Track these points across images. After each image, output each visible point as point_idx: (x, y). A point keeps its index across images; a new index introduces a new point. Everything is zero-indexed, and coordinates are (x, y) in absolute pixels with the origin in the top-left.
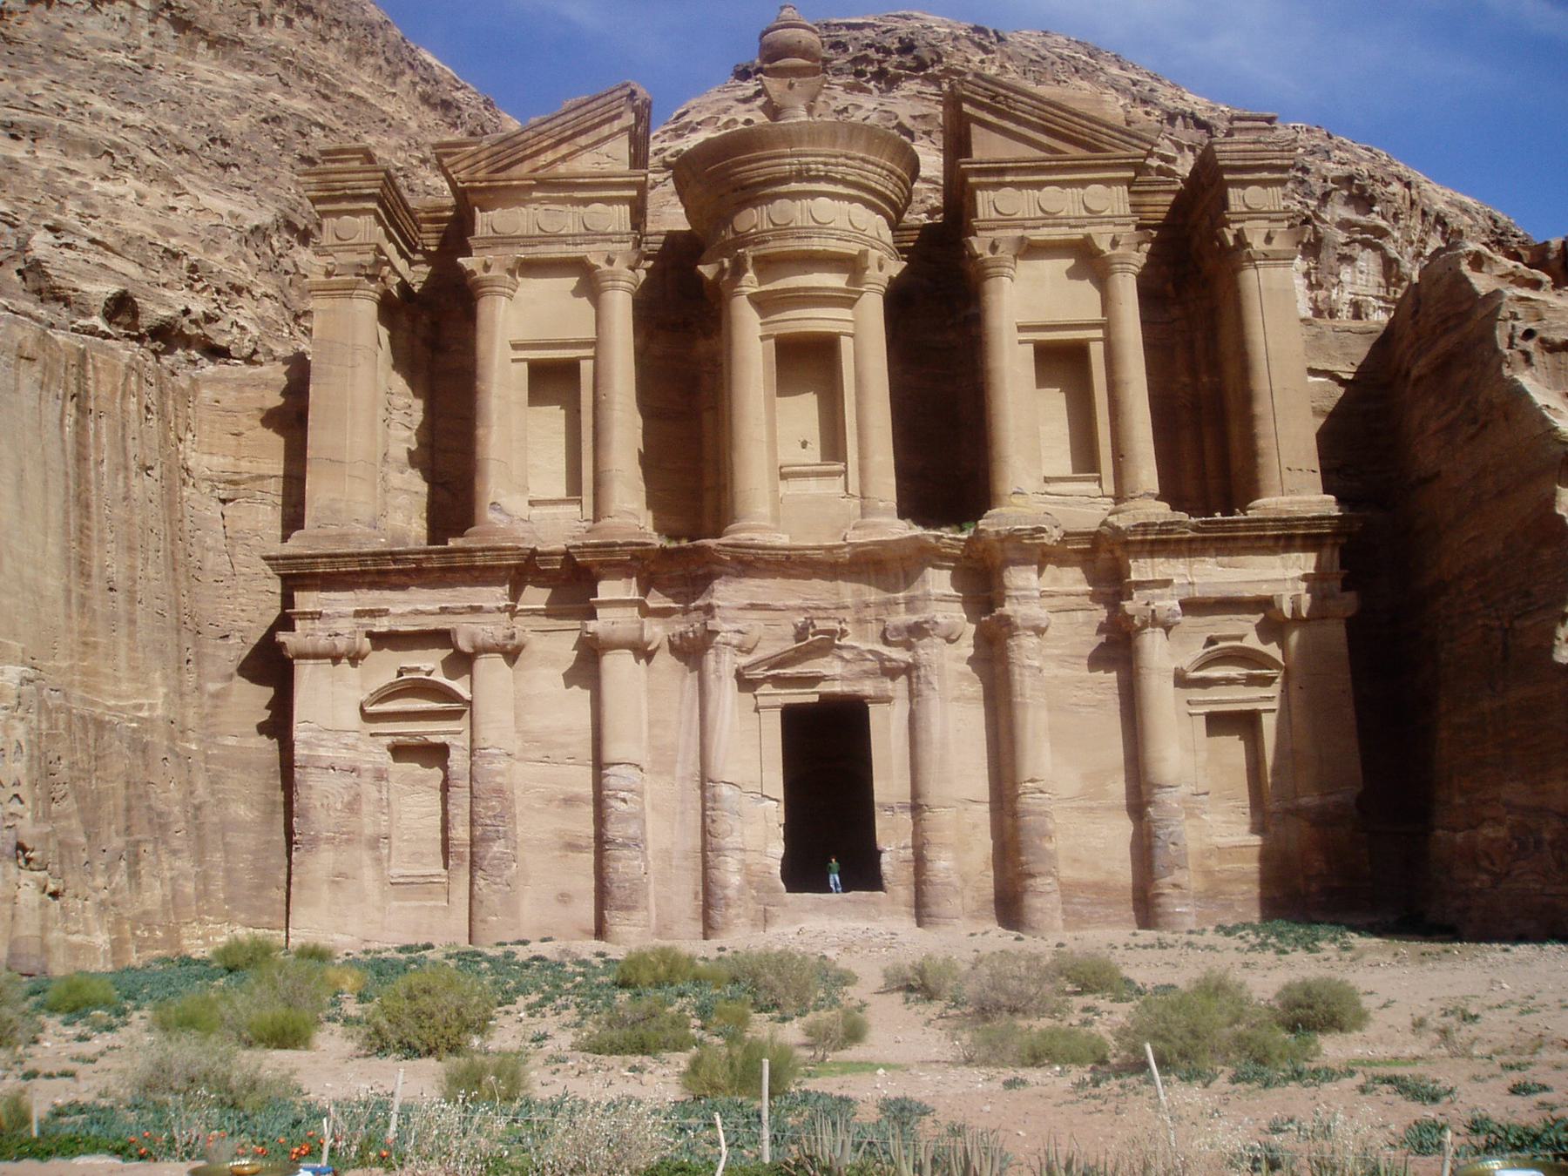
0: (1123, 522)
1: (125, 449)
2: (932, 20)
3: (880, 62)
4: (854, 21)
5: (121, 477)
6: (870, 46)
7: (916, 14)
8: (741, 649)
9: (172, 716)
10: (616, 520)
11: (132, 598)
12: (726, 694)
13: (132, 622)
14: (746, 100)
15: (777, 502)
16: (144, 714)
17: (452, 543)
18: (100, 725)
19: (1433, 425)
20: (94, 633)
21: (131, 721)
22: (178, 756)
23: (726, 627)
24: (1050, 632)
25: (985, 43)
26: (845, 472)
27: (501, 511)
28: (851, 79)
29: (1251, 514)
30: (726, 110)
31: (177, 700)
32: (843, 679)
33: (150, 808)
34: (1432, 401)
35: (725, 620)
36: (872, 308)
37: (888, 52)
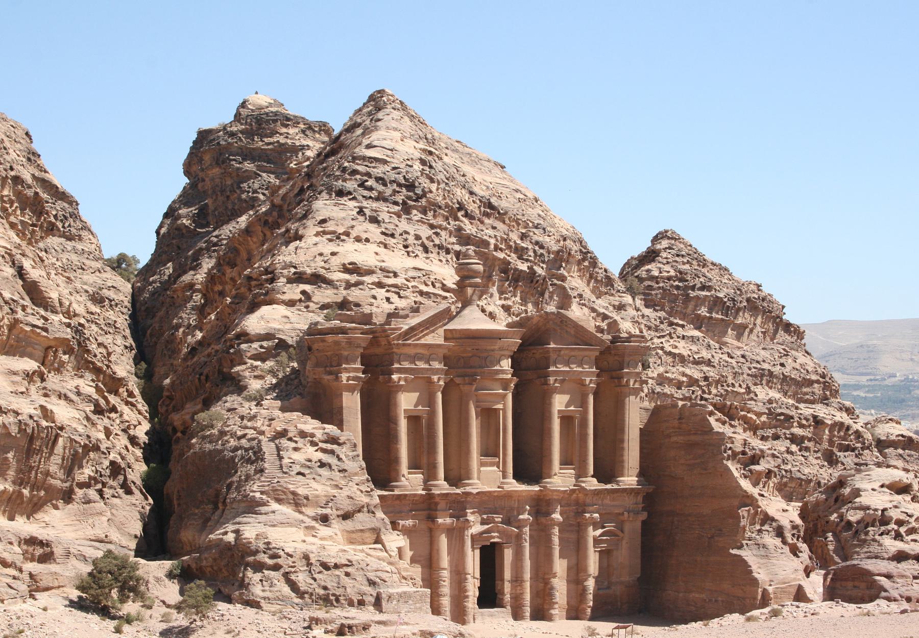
15: (479, 472)
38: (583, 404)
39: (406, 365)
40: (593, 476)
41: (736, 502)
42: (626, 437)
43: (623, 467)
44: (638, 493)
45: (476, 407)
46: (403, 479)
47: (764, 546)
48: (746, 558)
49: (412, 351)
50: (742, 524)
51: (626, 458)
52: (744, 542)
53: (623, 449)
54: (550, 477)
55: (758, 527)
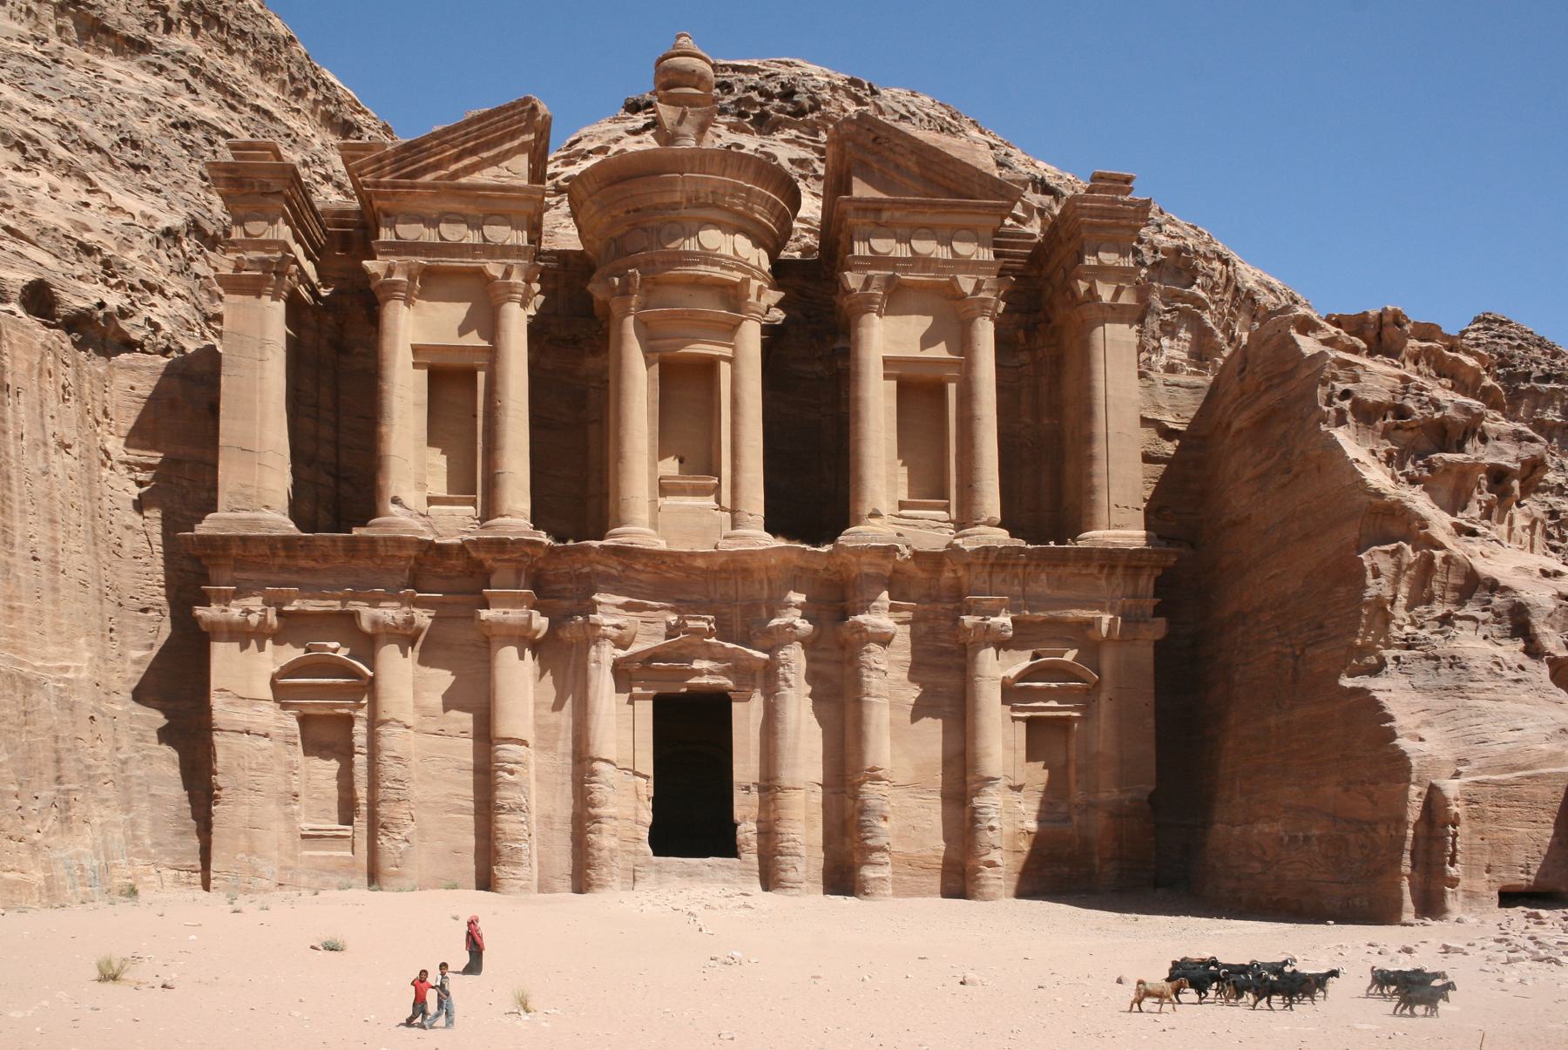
0: (967, 545)
1: (43, 426)
2: (812, 68)
3: (761, 105)
4: (740, 63)
5: (40, 453)
6: (753, 88)
7: (797, 61)
8: (621, 643)
9: (97, 679)
10: (507, 519)
11: (54, 566)
12: (603, 682)
13: (55, 590)
14: (635, 133)
15: (656, 510)
16: (70, 675)
17: (356, 532)
18: (27, 682)
19: (1248, 473)
20: (19, 598)
21: (59, 681)
22: (104, 715)
23: (606, 621)
24: (895, 641)
25: (861, 94)
26: (719, 486)
27: (402, 505)
28: (734, 119)
29: (1080, 545)
30: (617, 140)
31: (102, 665)
32: (710, 673)
33: (79, 760)
34: (1249, 451)
35: (605, 614)
36: (751, 337)
37: (769, 96)
38: (964, 345)
39: (411, 232)
40: (1000, 526)
41: (1351, 533)
42: (1099, 429)
43: (1091, 504)
44: (1138, 569)
45: (647, 352)
46: (393, 508)
47: (1455, 662)
48: (1379, 696)
49: (434, 207)
50: (1371, 592)
51: (1099, 481)
52: (1389, 654)
53: (1091, 459)
54: (858, 523)
55: (1439, 610)
